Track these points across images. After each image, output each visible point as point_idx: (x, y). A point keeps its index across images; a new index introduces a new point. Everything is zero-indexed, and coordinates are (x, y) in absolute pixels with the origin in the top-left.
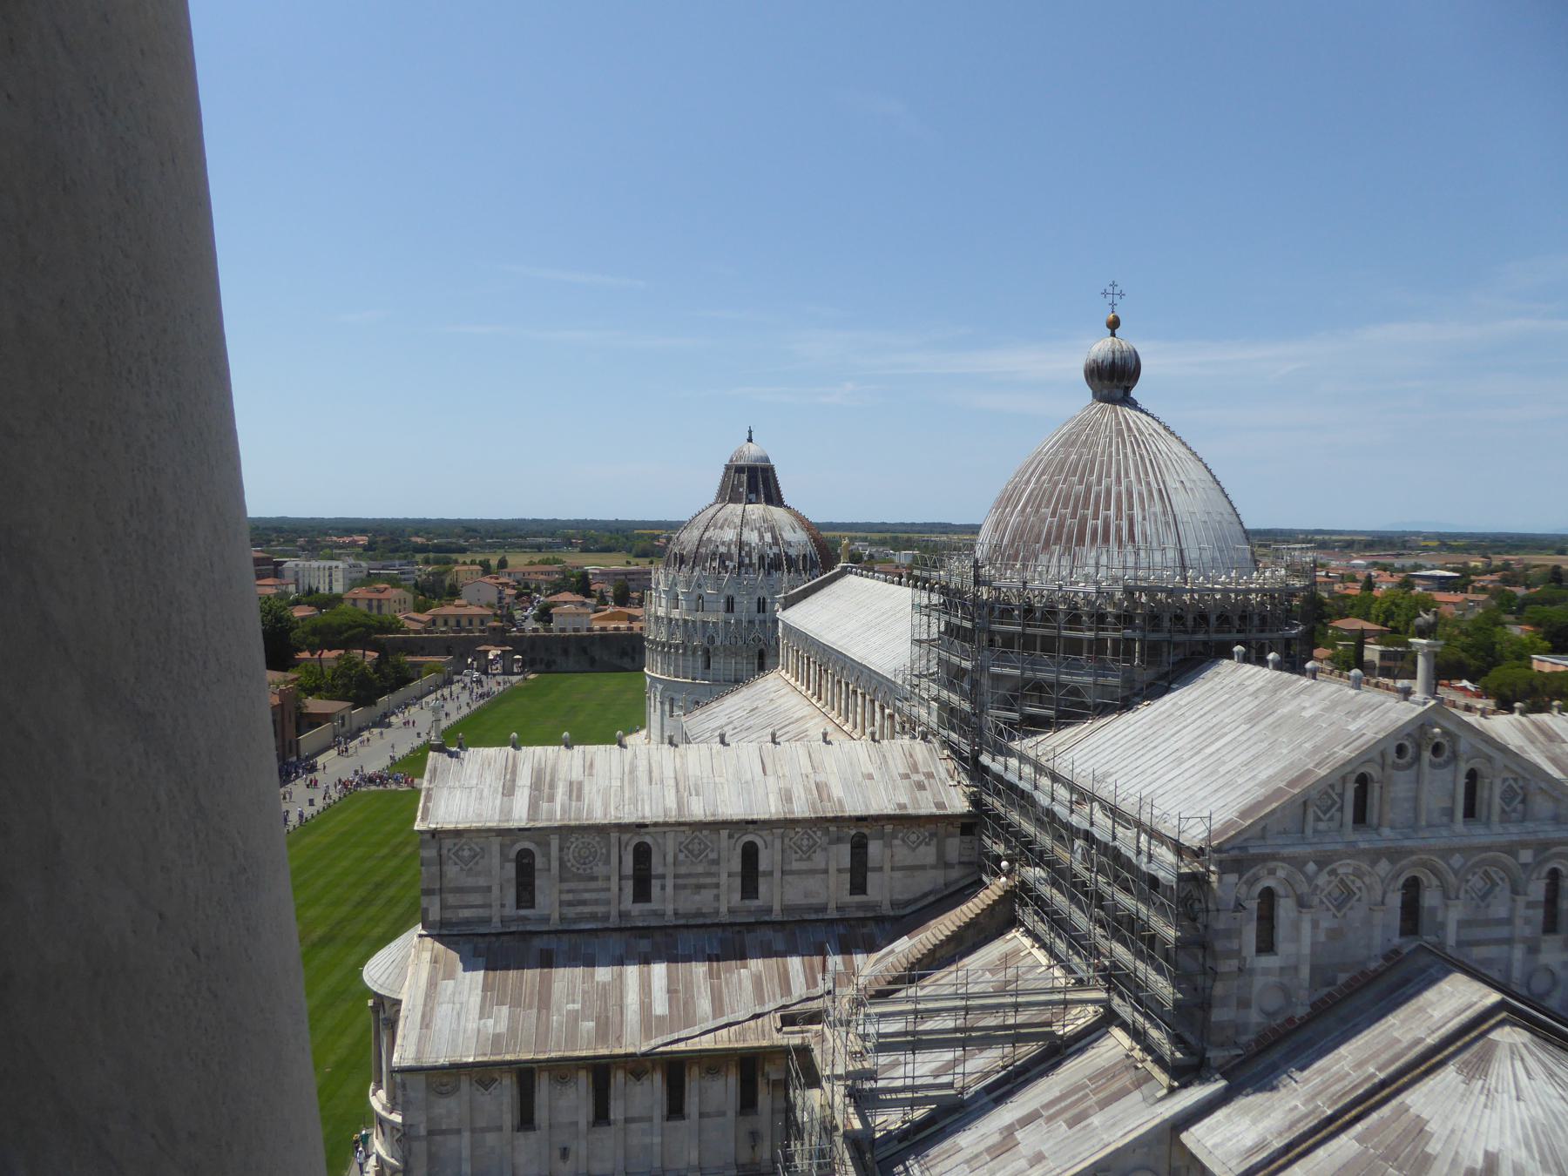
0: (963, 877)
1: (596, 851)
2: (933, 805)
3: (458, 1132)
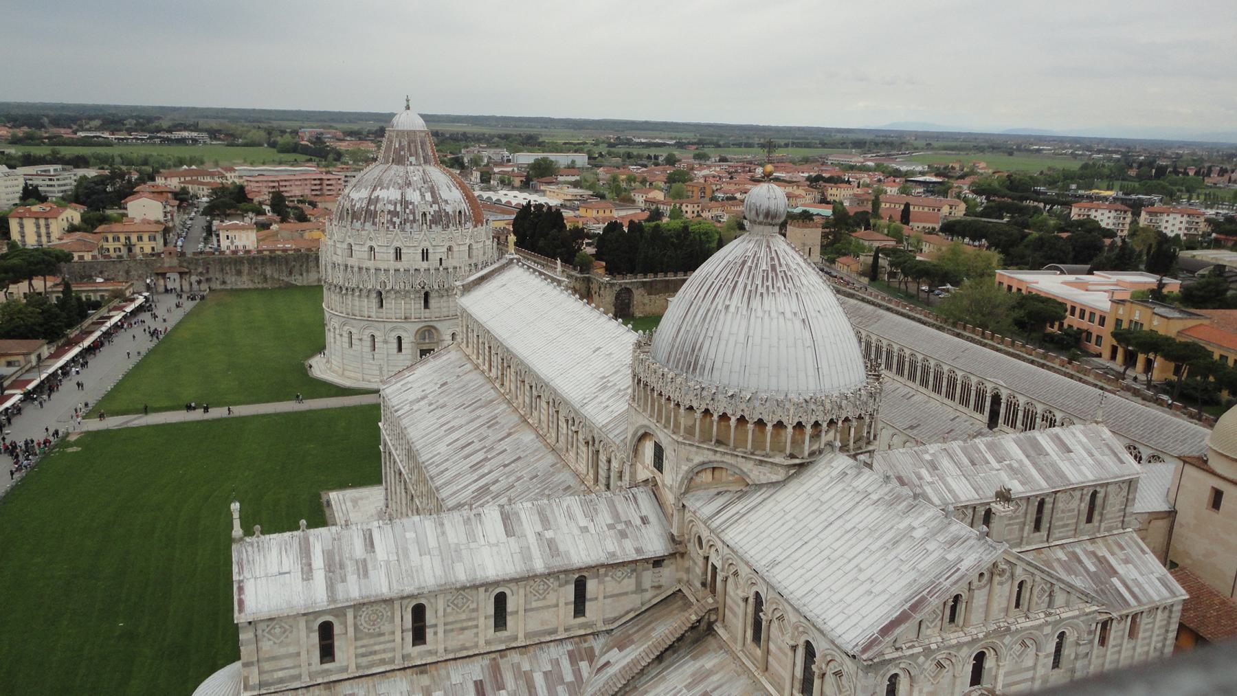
0: (654, 597)
1: (383, 615)
2: (634, 552)
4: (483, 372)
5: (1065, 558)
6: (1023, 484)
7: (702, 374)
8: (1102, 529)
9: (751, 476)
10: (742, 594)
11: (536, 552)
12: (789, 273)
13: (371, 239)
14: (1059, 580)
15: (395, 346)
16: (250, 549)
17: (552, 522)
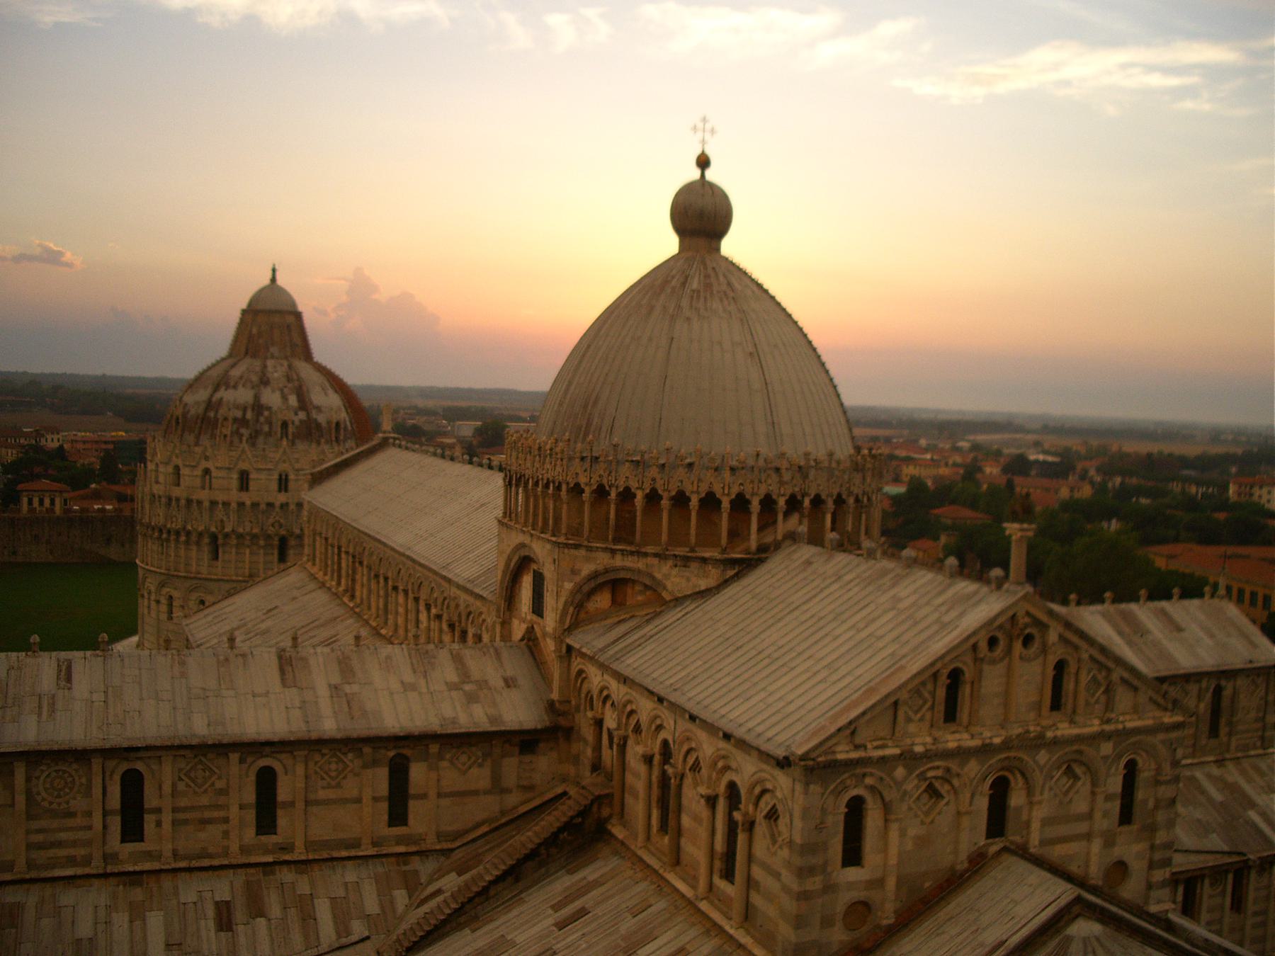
4: (329, 589)
8: (1233, 747)
9: (669, 585)
10: (640, 750)
12: (732, 294)
13: (207, 458)
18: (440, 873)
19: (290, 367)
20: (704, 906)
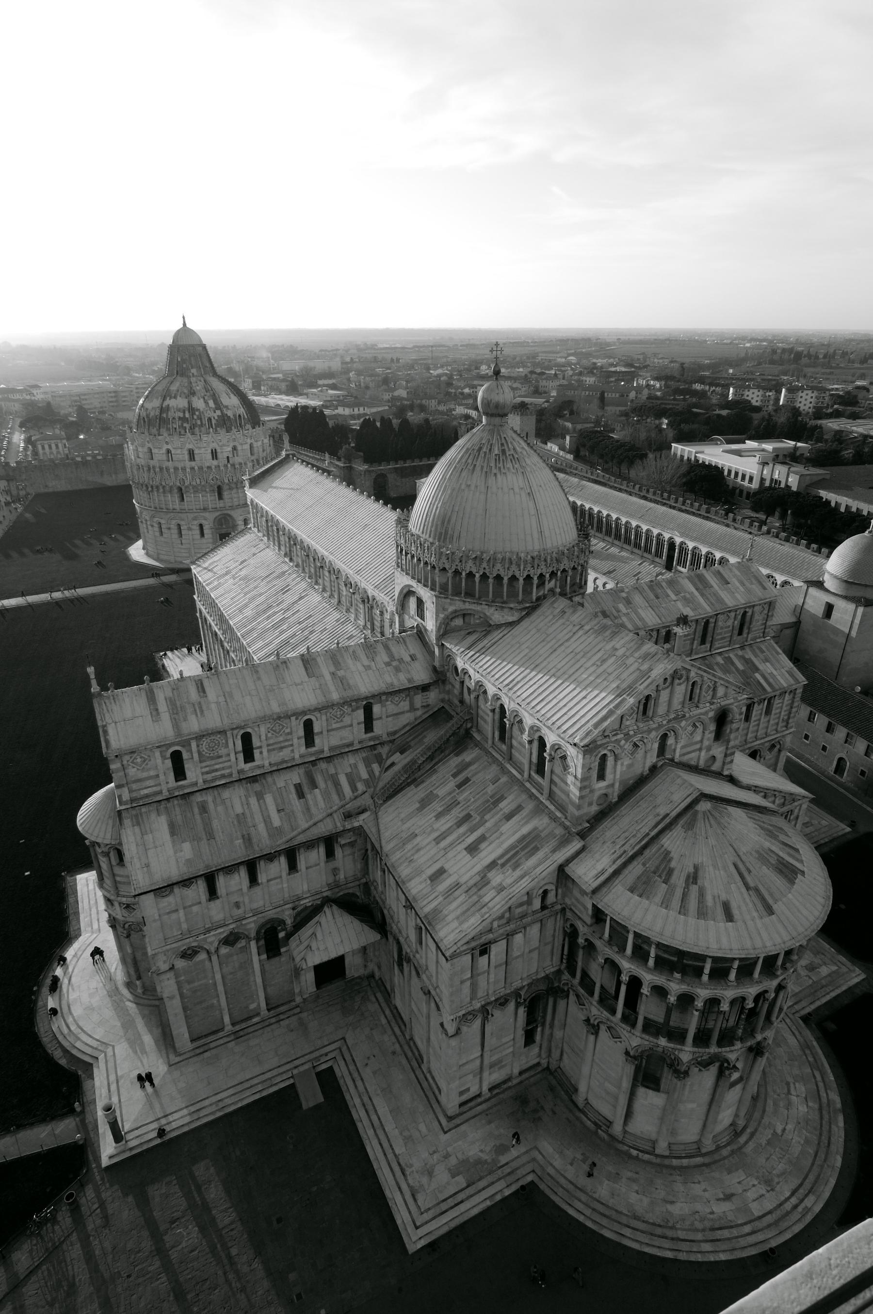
3: (177, 910)
5: (722, 662)
6: (693, 610)
7: (451, 542)
9: (493, 618)
11: (332, 688)
12: (516, 456)
13: (167, 443)
14: (720, 678)
15: (198, 532)
16: (107, 701)
17: (343, 665)
18: (391, 753)
19: (205, 381)
20: (528, 785)
